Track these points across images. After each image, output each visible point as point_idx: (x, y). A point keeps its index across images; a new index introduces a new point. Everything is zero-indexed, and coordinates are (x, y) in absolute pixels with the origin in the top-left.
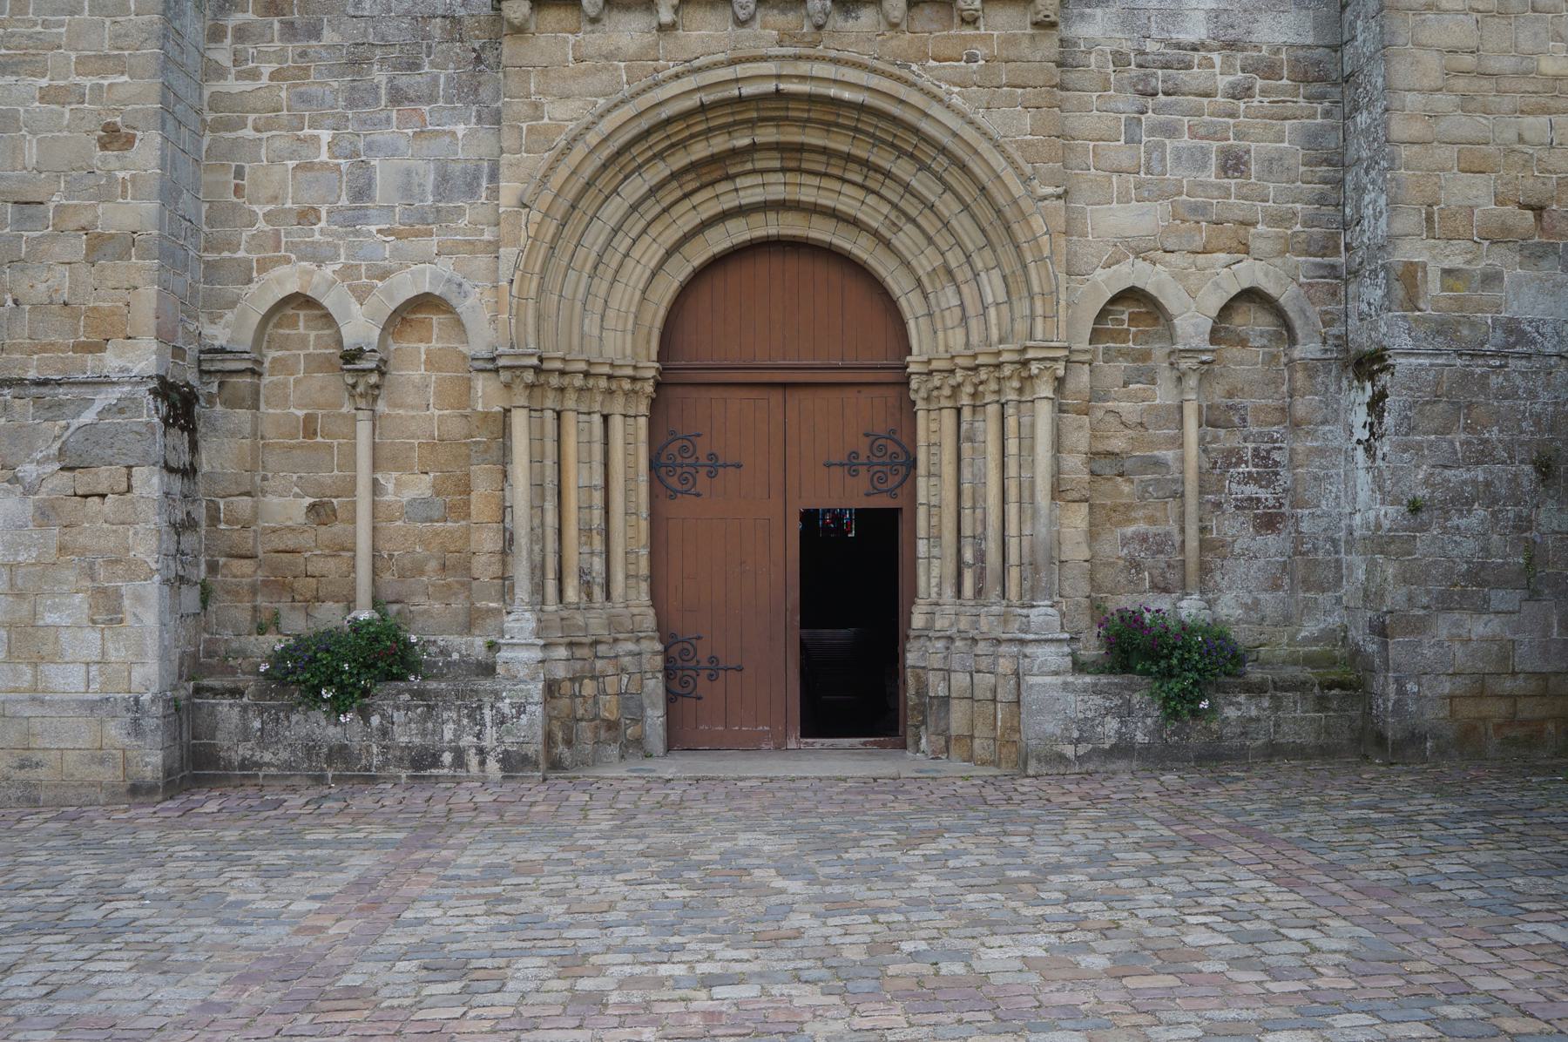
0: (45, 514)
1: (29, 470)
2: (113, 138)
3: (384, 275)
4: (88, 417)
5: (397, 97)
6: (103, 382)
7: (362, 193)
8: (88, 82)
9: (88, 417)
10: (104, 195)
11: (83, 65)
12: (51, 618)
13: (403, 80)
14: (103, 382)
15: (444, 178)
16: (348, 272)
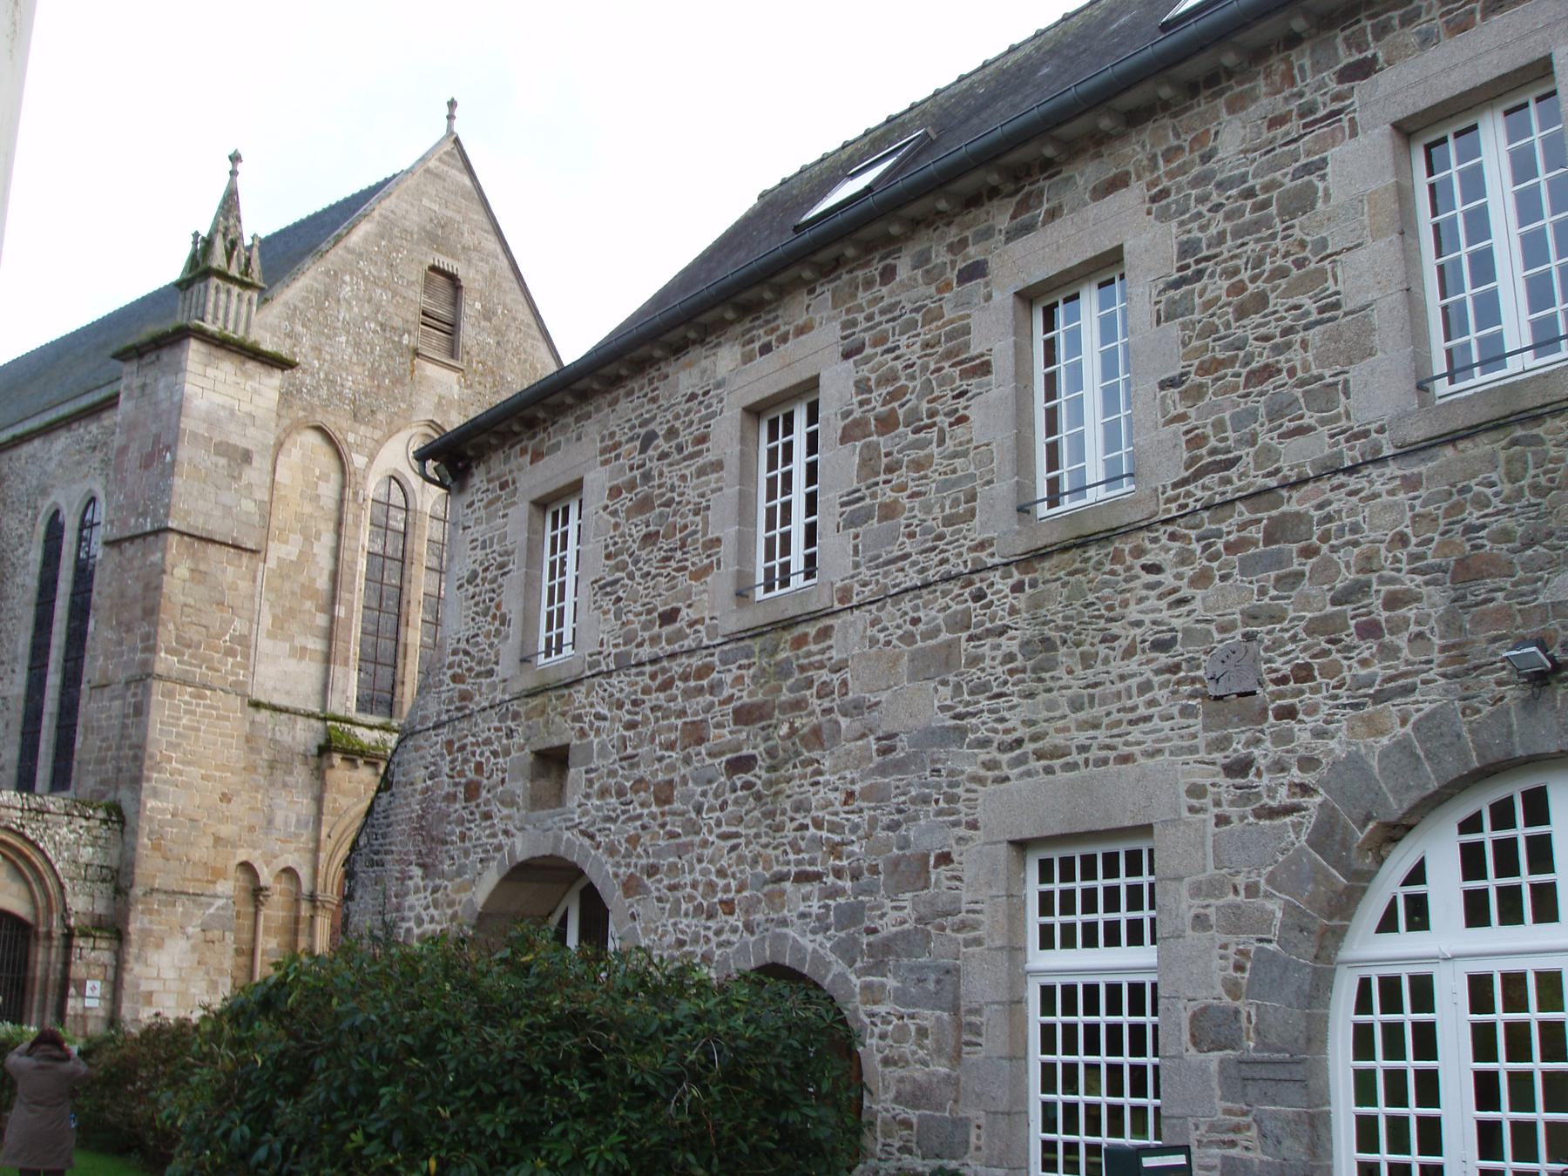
0: (194, 948)
1: (190, 930)
2: (226, 798)
3: (276, 857)
4: (212, 910)
5: (285, 785)
6: (215, 896)
7: (270, 822)
8: (218, 774)
9: (212, 910)
10: (220, 821)
11: (217, 767)
12: (193, 990)
13: (287, 779)
14: (215, 896)
15: (298, 821)
16: (263, 854)
